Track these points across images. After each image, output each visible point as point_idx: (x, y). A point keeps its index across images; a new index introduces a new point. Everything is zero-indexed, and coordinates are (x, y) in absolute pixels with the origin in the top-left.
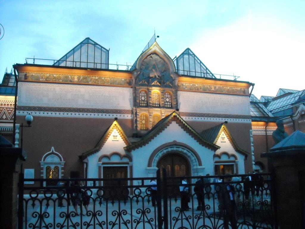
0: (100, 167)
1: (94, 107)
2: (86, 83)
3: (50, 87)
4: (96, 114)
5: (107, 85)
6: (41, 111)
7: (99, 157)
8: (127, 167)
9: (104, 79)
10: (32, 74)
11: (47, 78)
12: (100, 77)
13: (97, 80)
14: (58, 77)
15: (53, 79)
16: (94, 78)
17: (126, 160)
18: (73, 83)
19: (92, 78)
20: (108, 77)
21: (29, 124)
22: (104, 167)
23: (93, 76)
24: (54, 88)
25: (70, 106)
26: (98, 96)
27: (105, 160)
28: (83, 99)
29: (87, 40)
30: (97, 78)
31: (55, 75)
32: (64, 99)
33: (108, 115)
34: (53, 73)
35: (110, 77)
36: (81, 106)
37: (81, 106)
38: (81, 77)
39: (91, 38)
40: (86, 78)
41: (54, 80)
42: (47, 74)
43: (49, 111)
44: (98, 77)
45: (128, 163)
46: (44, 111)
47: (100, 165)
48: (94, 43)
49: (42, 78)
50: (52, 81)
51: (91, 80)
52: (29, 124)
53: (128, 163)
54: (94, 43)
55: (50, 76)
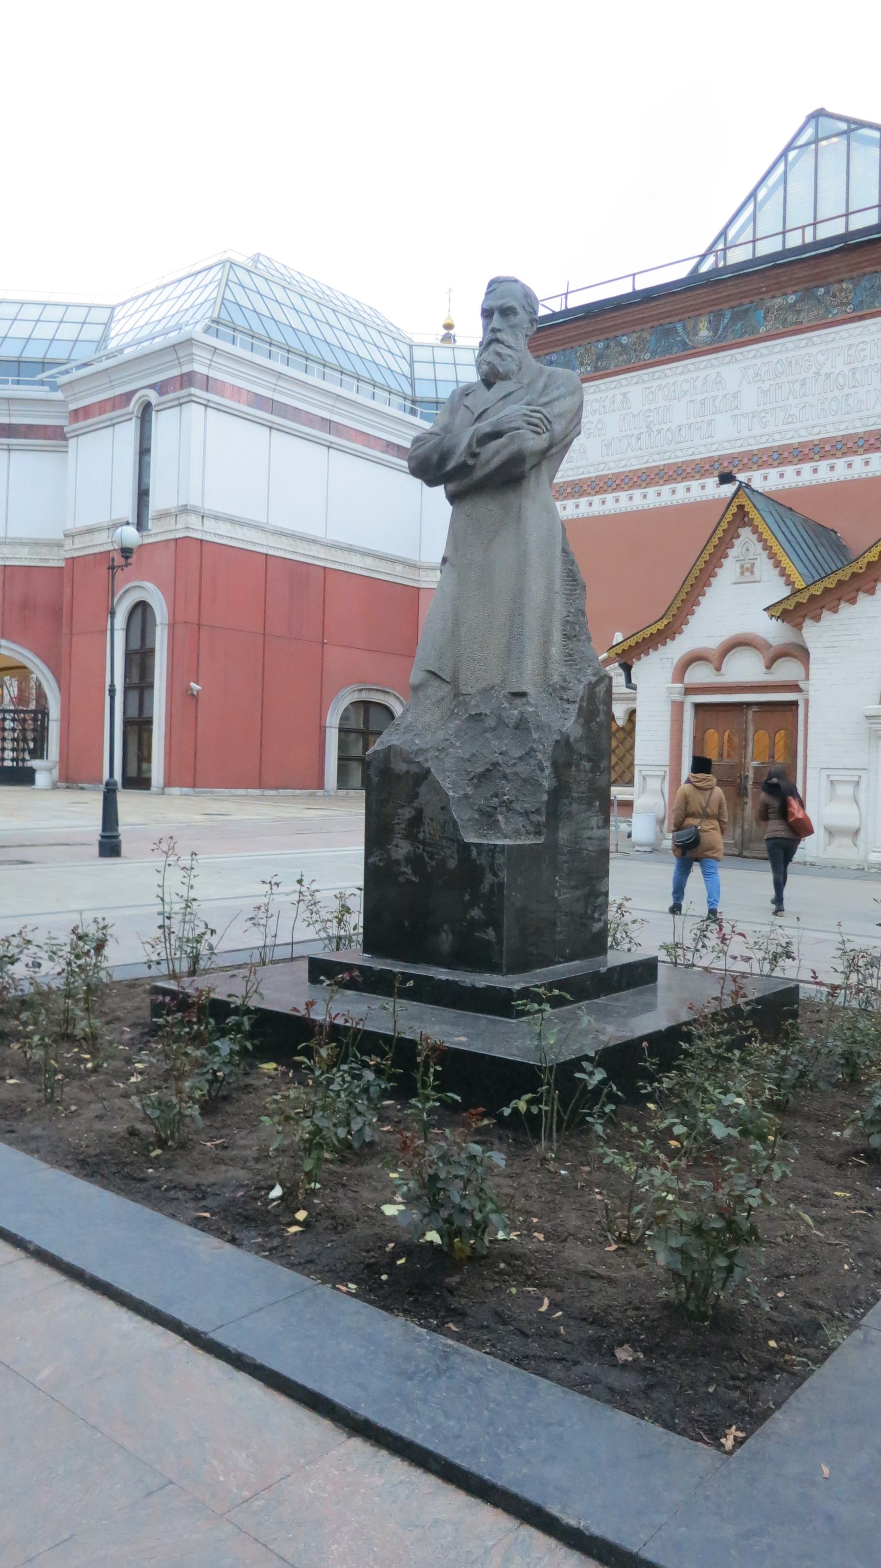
0: (678, 707)
1: (779, 441)
2: (746, 338)
3: (610, 394)
4: (789, 470)
5: (839, 317)
6: (581, 495)
7: (676, 661)
8: (795, 704)
9: (827, 292)
10: (548, 357)
11: (598, 359)
12: (807, 289)
13: (793, 305)
14: (635, 344)
15: (621, 355)
16: (779, 300)
17: (787, 671)
18: (693, 351)
19: (769, 304)
20: (841, 281)
21: (127, 558)
22: (698, 706)
23: (773, 297)
24: (624, 394)
25: (681, 457)
26: (797, 386)
27: (700, 675)
28: (735, 412)
29: (813, 122)
30: (792, 299)
31: (624, 340)
32: (659, 432)
33: (840, 463)
34: (617, 333)
35: (855, 274)
36: (727, 445)
37: (727, 445)
38: (723, 315)
39: (831, 109)
40: (747, 311)
41: (621, 359)
42: (598, 341)
43: (606, 491)
44: (794, 292)
45: (794, 687)
46: (589, 494)
47: (678, 698)
48: (843, 126)
49: (582, 364)
50: (616, 366)
51: (765, 318)
52: (127, 558)
53: (794, 687)
54: (843, 126)
55: (608, 347)
